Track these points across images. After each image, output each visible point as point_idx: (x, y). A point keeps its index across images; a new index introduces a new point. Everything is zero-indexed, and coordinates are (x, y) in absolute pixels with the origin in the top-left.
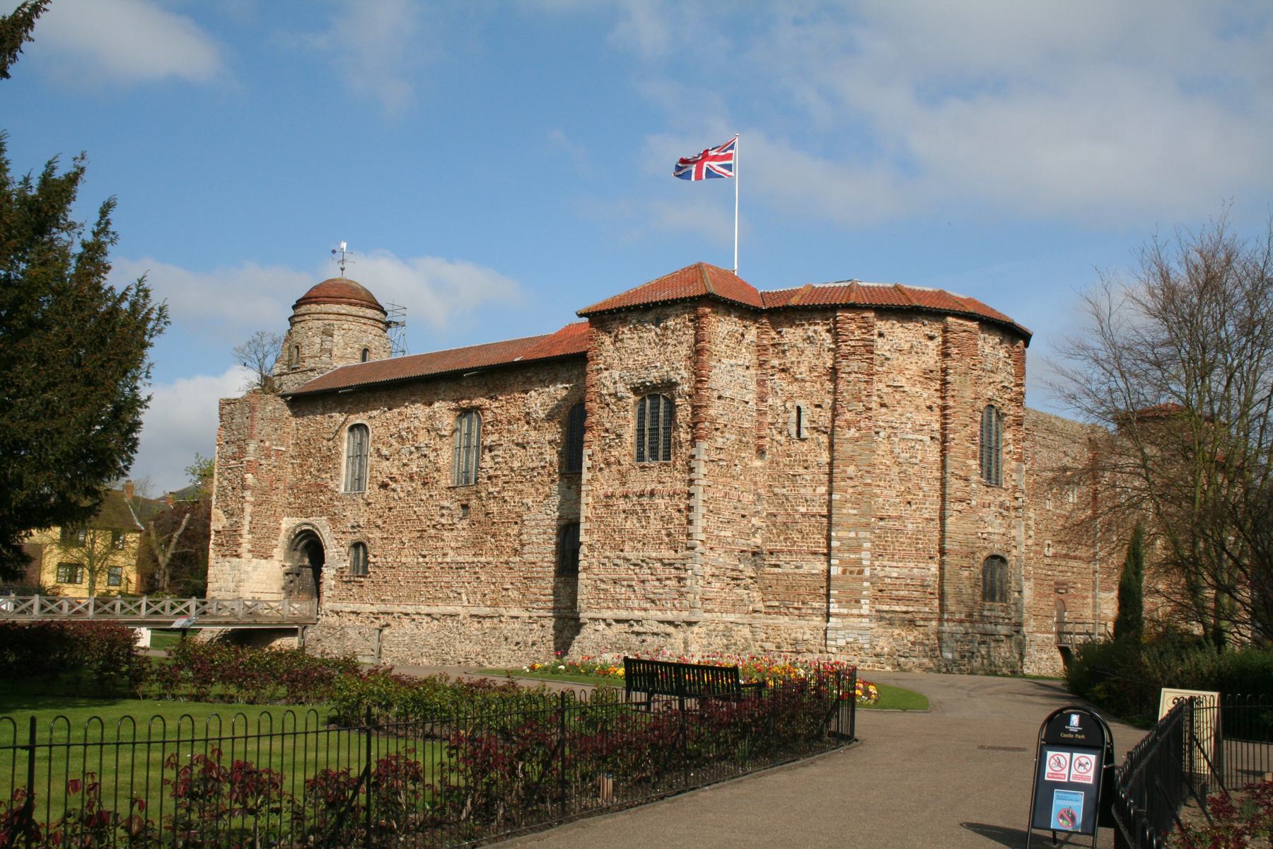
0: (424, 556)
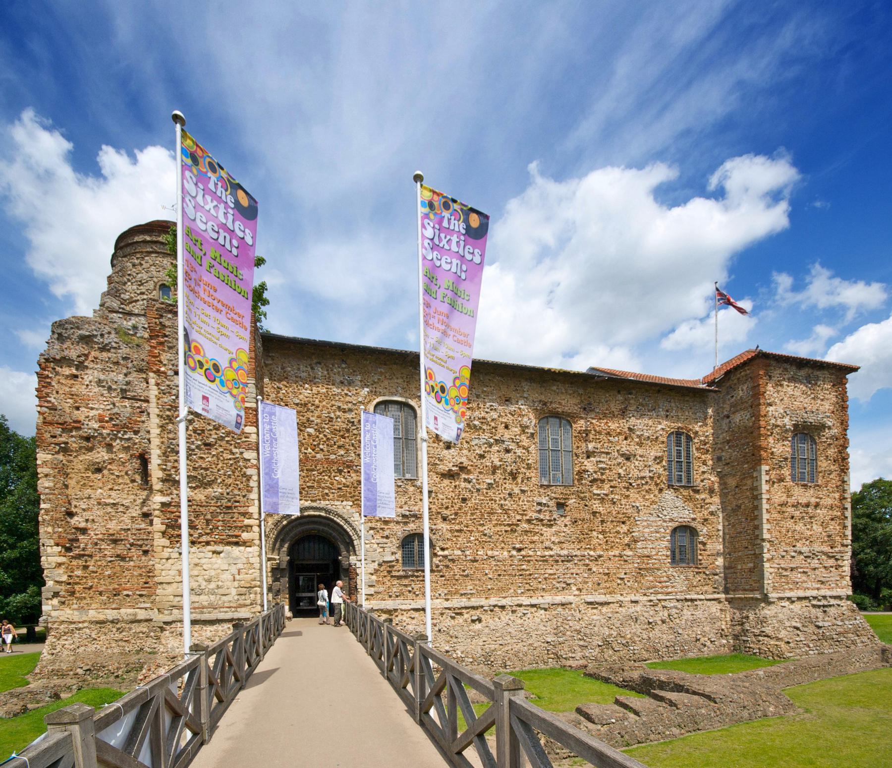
0: (519, 550)
